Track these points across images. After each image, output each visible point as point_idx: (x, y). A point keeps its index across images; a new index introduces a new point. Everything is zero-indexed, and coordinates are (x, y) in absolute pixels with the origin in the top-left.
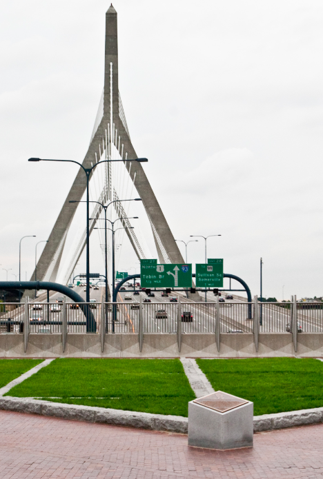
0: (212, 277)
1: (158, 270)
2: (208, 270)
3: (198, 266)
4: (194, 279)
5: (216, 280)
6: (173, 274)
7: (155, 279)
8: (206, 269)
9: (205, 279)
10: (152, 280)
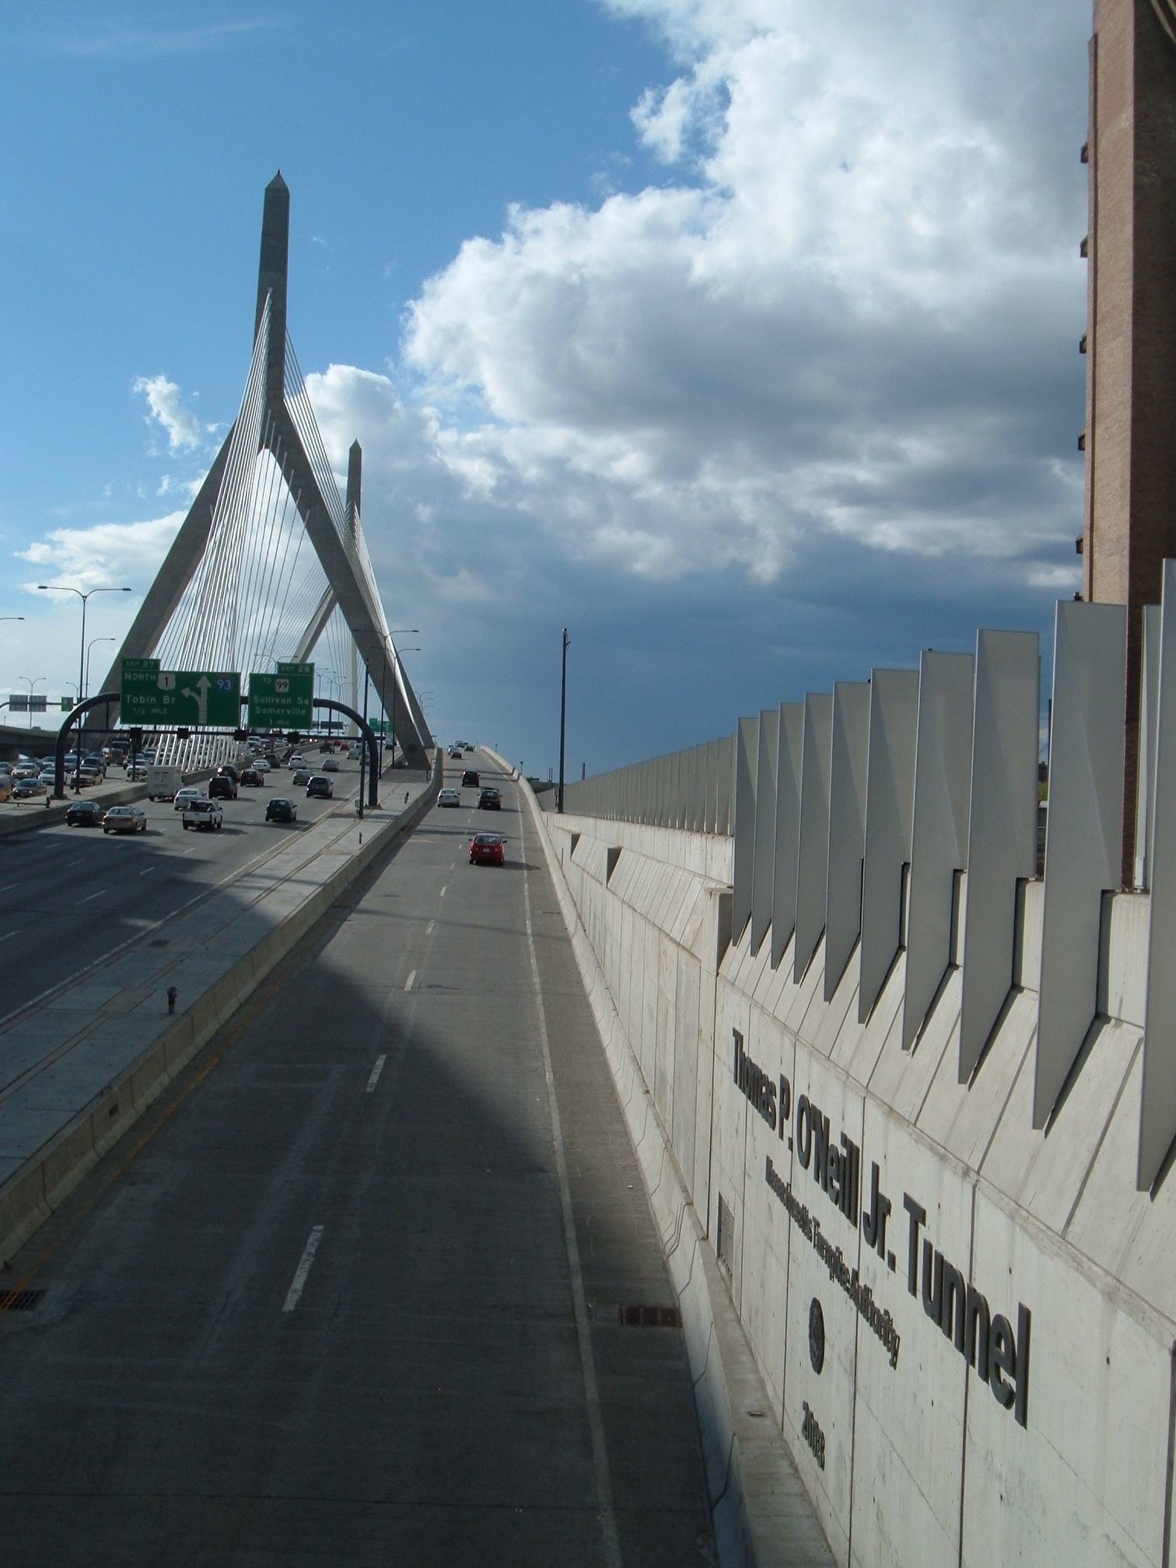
0: (284, 706)
1: (161, 685)
2: (278, 690)
3: (255, 679)
4: (244, 710)
5: (296, 711)
6: (196, 697)
7: (154, 706)
8: (273, 683)
9: (271, 711)
10: (148, 706)
